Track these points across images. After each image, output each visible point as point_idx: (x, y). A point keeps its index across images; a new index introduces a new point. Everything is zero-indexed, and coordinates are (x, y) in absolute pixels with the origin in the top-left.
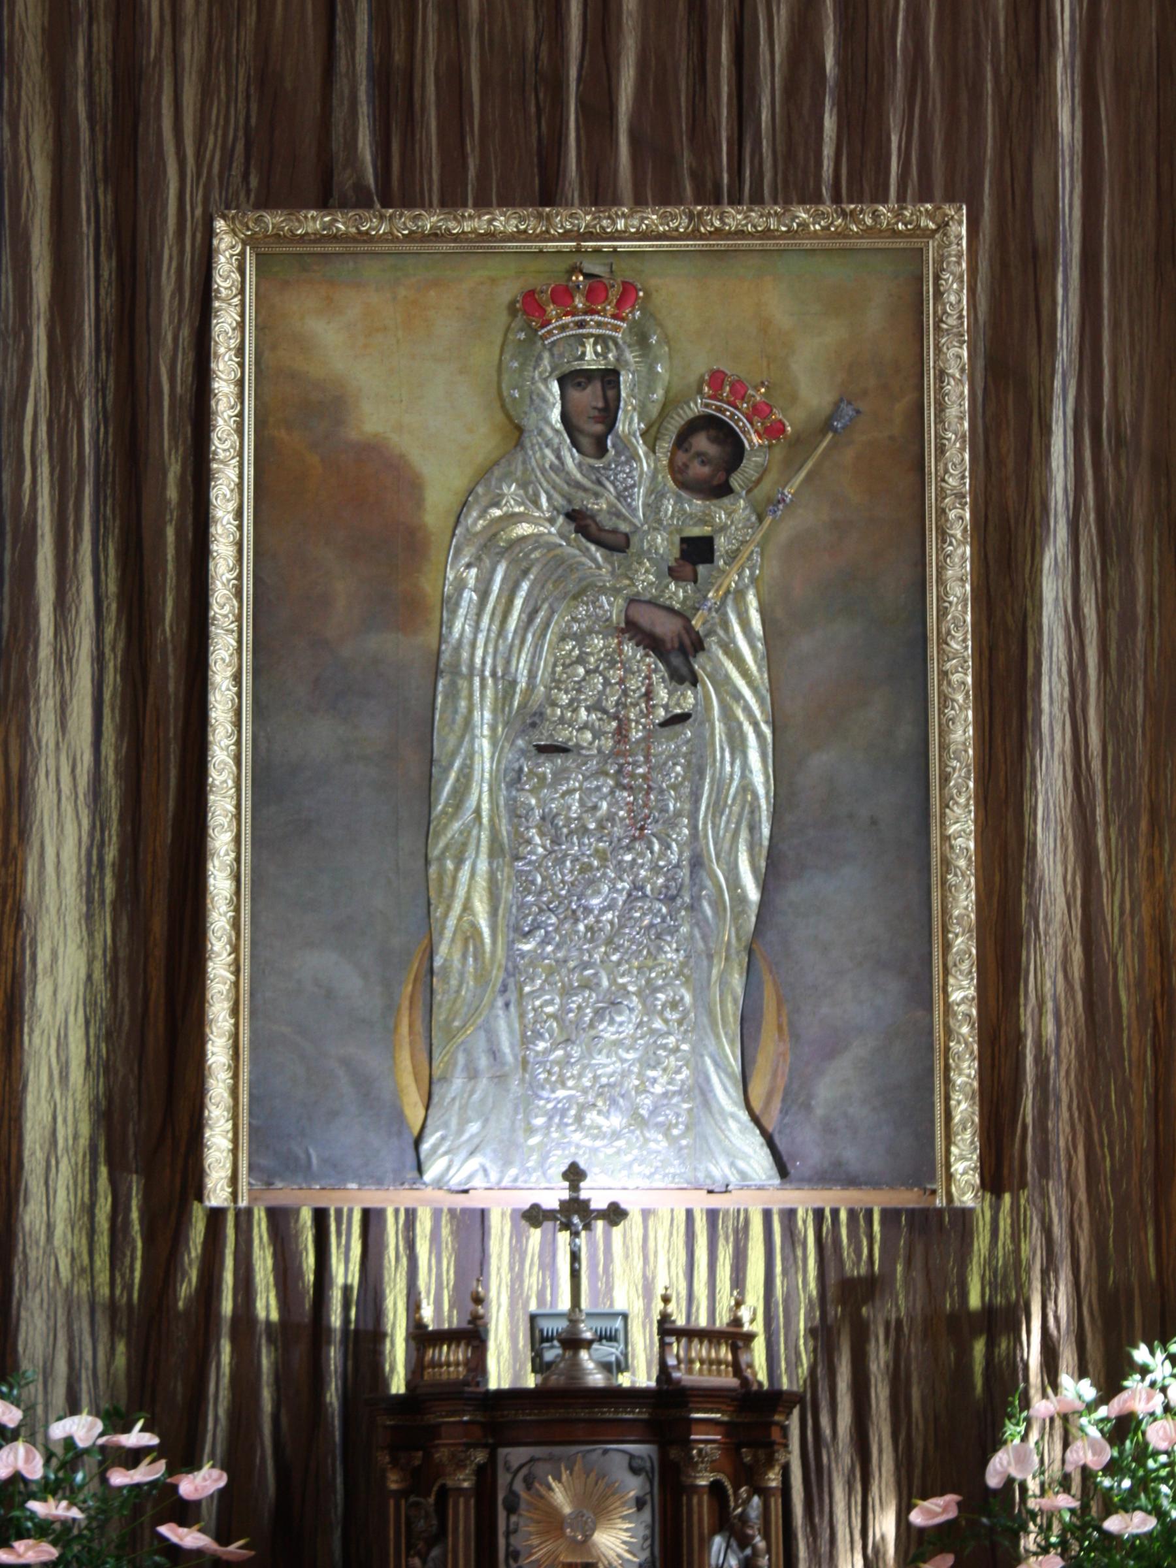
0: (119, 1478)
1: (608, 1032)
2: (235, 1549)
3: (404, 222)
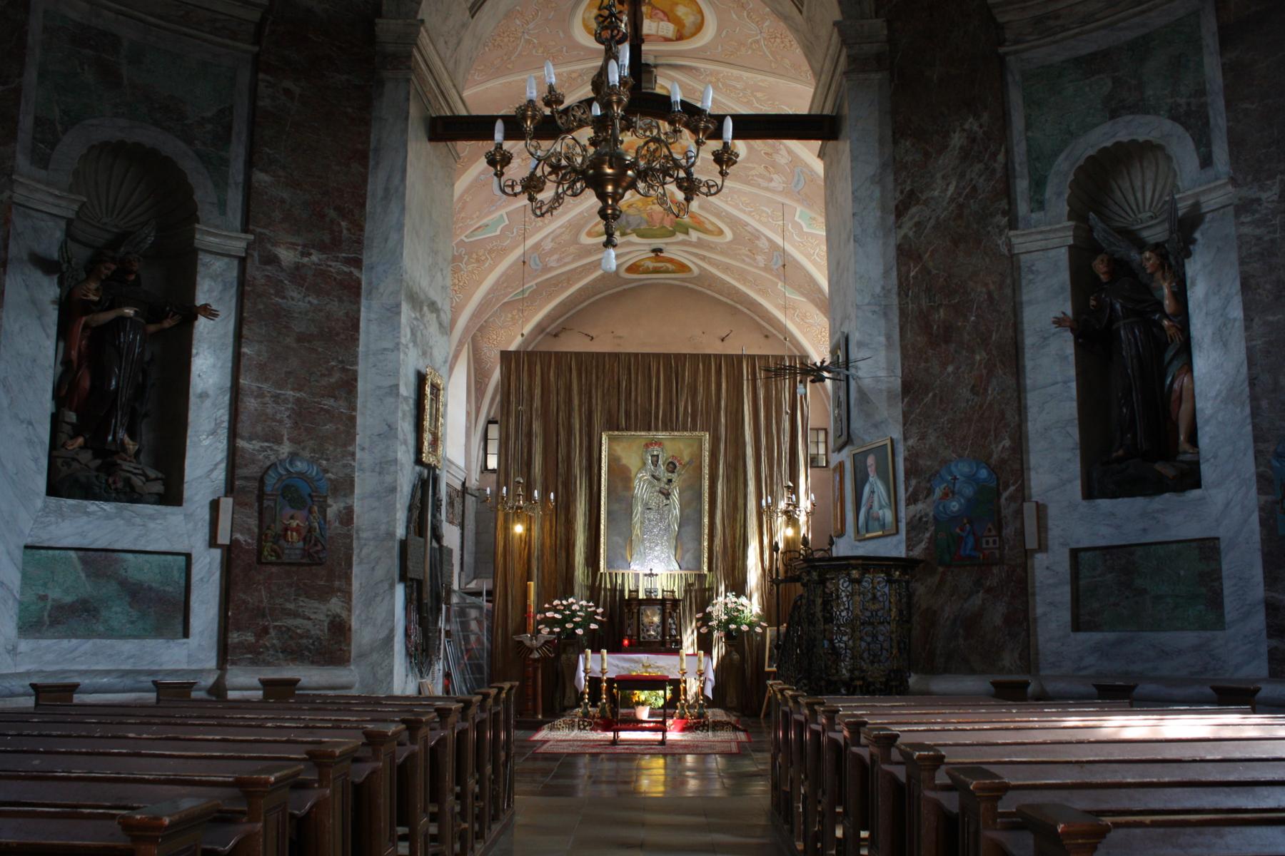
0: (589, 610)
1: (656, 549)
2: (605, 619)
3: (629, 433)
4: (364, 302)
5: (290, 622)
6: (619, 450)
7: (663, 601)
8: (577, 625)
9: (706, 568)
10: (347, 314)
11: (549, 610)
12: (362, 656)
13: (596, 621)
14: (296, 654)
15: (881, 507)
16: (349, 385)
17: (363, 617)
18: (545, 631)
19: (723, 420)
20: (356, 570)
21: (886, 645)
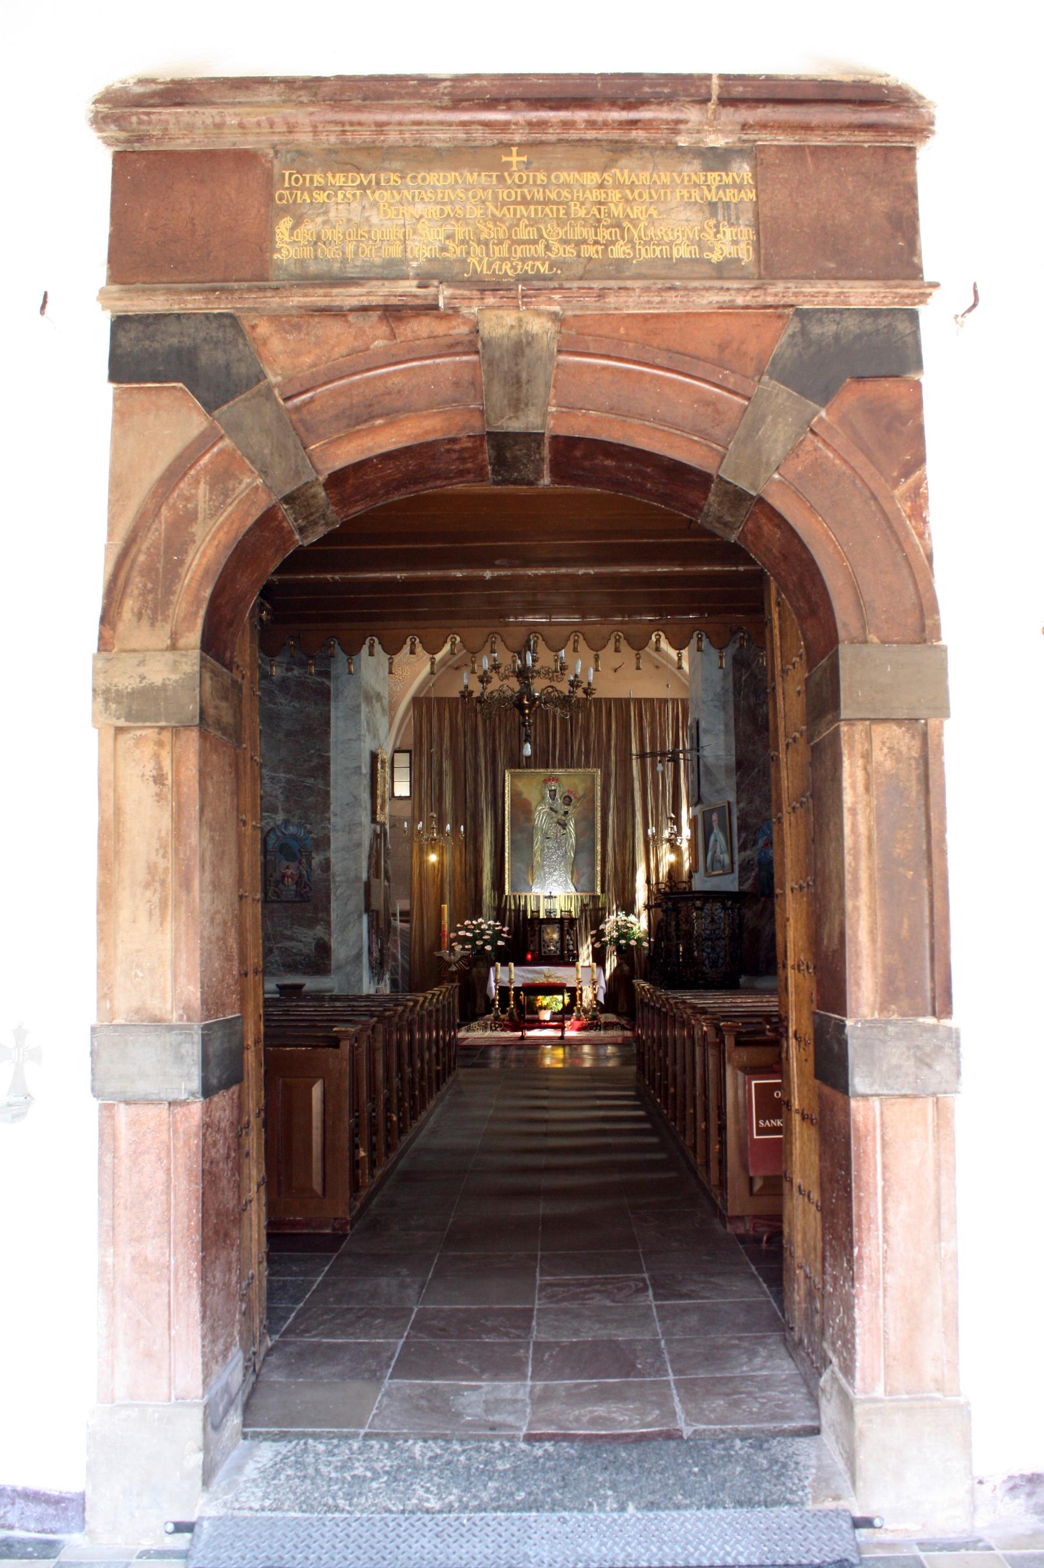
4: (332, 703)
5: (288, 944)
6: (521, 785)
7: (561, 920)
8: (486, 942)
9: (599, 890)
10: (321, 715)
11: (461, 929)
12: (339, 968)
13: (502, 939)
14: (292, 967)
15: (722, 853)
16: (323, 768)
17: (339, 939)
18: (458, 948)
19: (613, 758)
20: (333, 905)
21: (722, 954)
